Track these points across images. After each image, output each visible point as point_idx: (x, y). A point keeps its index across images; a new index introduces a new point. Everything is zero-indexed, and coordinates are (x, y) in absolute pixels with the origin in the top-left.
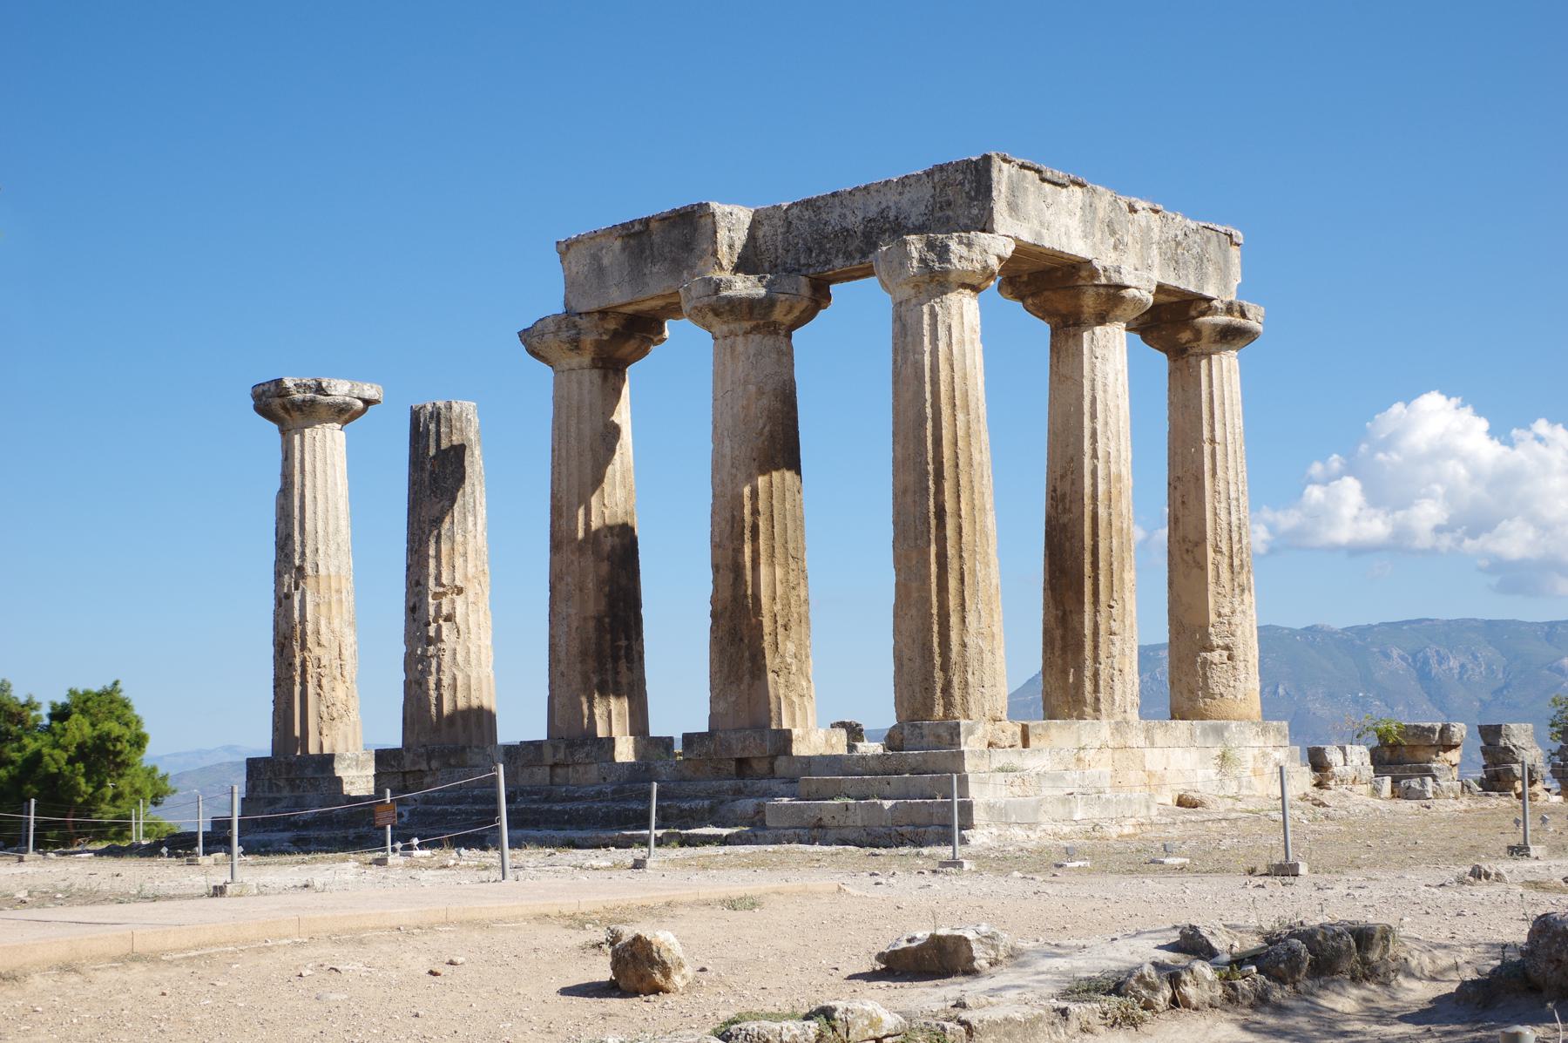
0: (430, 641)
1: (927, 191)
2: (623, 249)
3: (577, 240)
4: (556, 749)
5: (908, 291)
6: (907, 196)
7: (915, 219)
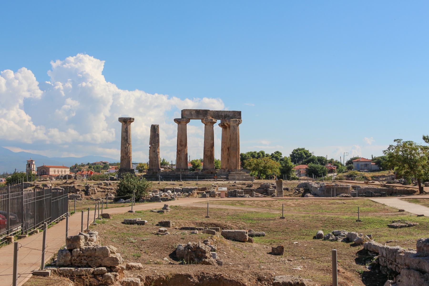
1: (232, 113)
7: (231, 116)
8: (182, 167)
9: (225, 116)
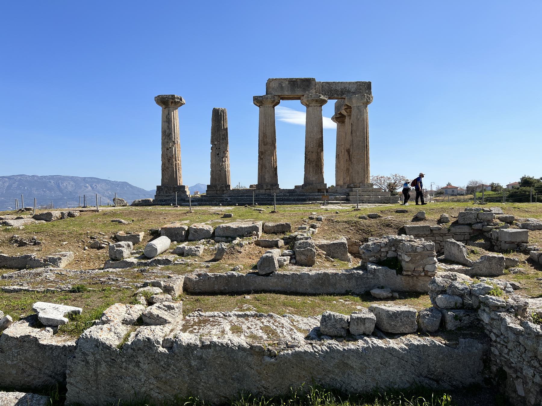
0: (223, 162)
1: (355, 86)
2: (289, 84)
3: (276, 79)
4: (267, 186)
5: (362, 104)
6: (350, 86)
7: (353, 90)
8: (267, 180)
9: (342, 92)
